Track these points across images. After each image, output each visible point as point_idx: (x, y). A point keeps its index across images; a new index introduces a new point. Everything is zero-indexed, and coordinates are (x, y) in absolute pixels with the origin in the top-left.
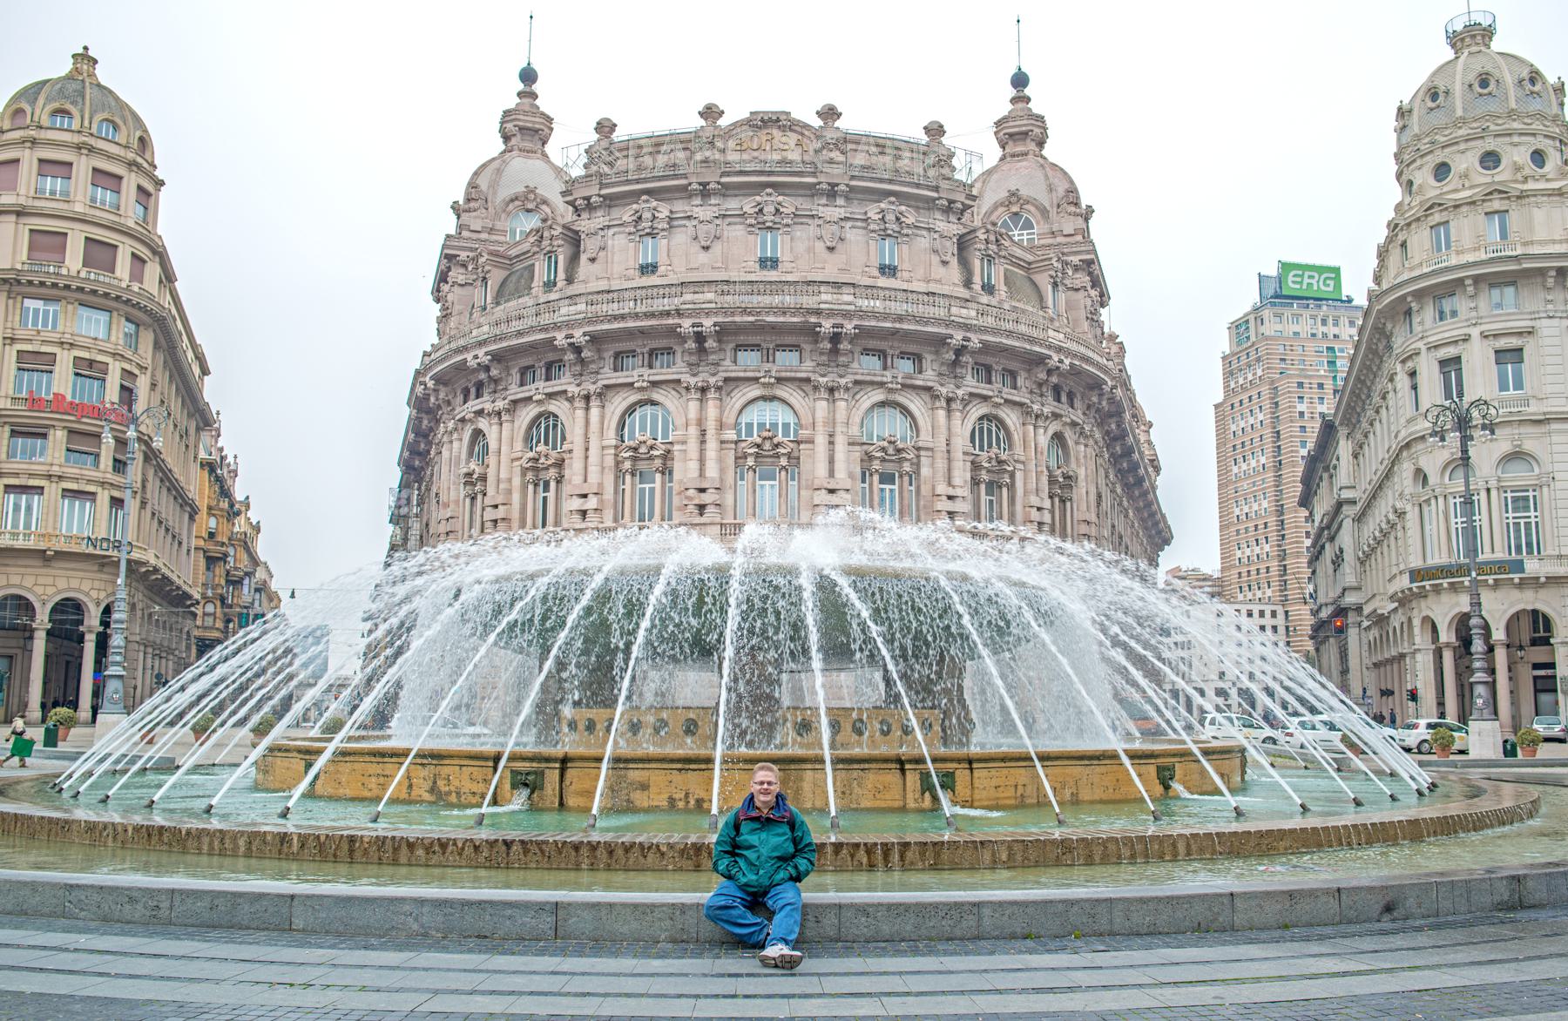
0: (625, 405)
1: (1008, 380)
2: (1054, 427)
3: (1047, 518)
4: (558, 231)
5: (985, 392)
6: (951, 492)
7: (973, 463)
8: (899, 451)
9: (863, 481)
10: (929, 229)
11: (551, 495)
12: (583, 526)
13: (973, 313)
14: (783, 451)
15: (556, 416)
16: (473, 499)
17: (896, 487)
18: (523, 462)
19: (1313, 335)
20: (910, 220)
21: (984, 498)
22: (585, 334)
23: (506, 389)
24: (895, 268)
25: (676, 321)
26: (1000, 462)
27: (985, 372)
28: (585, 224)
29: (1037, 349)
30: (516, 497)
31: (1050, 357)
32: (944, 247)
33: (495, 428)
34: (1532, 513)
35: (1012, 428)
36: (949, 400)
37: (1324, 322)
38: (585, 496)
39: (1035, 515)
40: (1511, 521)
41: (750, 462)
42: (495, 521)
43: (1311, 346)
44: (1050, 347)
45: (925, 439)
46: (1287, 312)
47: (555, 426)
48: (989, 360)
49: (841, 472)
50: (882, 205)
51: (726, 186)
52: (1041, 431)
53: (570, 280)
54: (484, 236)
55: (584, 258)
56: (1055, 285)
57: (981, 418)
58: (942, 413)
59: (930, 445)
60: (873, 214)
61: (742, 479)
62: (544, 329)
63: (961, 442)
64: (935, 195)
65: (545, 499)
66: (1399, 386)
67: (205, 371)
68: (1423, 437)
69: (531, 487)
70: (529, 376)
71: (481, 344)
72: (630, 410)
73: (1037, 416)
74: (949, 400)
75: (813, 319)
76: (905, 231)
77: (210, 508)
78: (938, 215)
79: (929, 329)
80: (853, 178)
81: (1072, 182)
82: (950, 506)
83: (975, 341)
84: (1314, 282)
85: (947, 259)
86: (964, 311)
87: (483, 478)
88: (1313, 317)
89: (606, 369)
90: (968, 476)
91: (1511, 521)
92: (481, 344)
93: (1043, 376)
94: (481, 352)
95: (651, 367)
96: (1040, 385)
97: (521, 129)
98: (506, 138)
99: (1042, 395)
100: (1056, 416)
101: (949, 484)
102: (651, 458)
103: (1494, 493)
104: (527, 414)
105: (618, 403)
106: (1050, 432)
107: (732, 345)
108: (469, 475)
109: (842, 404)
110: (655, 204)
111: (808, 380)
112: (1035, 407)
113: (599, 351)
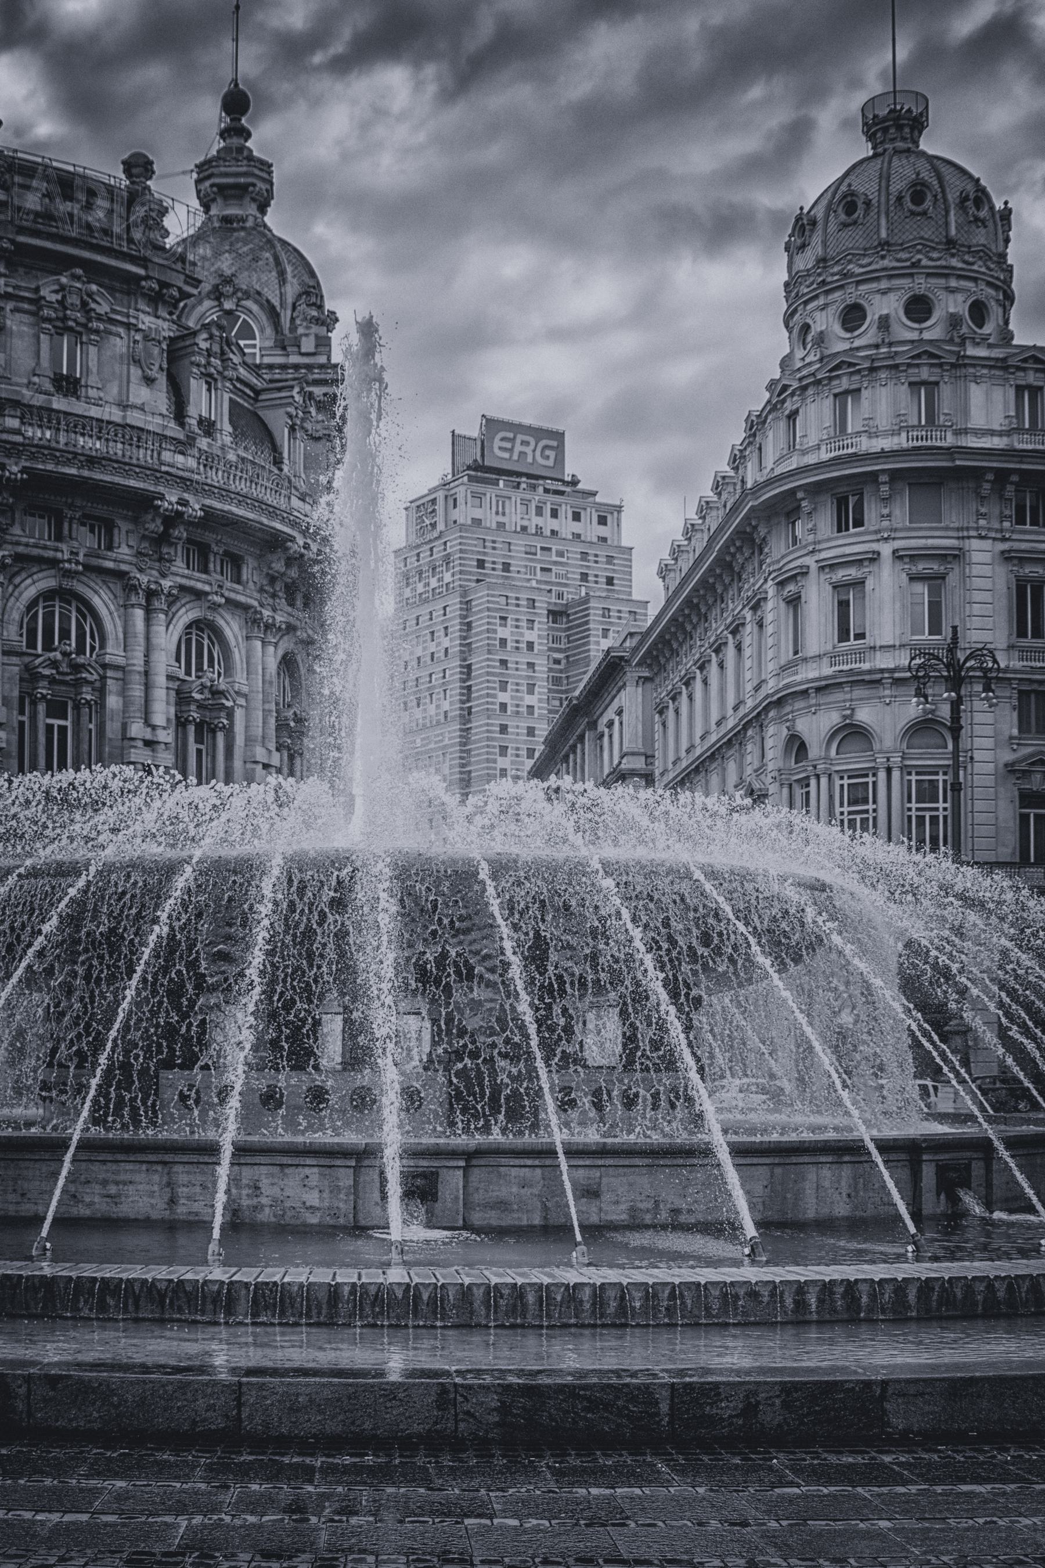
1: (228, 569)
5: (199, 586)
6: (148, 736)
7: (178, 692)
10: (128, 326)
13: (192, 463)
19: (524, 529)
20: (103, 308)
21: (192, 747)
24: (77, 381)
26: (216, 693)
27: (200, 555)
29: (279, 526)
32: (150, 355)
34: (941, 805)
35: (232, 642)
36: (151, 595)
37: (539, 512)
40: (913, 813)
43: (520, 544)
45: (114, 653)
46: (490, 492)
48: (209, 537)
50: (64, 280)
52: (271, 649)
56: (292, 429)
57: (189, 626)
58: (139, 614)
59: (121, 661)
63: (163, 663)
64: (142, 272)
66: (769, 617)
68: (805, 693)
73: (267, 627)
76: (94, 325)
78: (142, 306)
79: (132, 483)
80: (21, 230)
81: (312, 274)
83: (195, 507)
84: (528, 450)
85: (154, 373)
86: (180, 458)
88: (526, 503)
90: (172, 710)
91: (913, 813)
99: (274, 596)
101: (148, 723)
103: (896, 774)
112: (266, 613)
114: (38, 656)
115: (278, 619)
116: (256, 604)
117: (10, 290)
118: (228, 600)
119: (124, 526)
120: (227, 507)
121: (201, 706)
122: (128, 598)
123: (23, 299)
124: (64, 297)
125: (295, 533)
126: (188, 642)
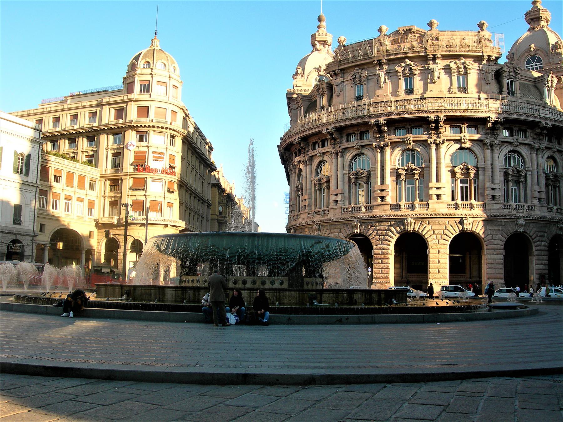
0: (352, 156)
2: (548, 154)
3: (543, 196)
4: (325, 85)
6: (493, 186)
12: (336, 207)
16: (299, 197)
17: (468, 185)
22: (333, 128)
23: (308, 151)
25: (368, 120)
26: (518, 171)
28: (335, 81)
30: (313, 195)
31: (541, 122)
32: (487, 77)
35: (525, 155)
38: (337, 195)
39: (536, 194)
41: (403, 177)
44: (540, 118)
51: (389, 60)
53: (330, 105)
55: (334, 95)
57: (509, 152)
58: (488, 152)
59: (483, 166)
60: (453, 65)
62: (318, 127)
64: (481, 54)
67: (211, 149)
70: (317, 146)
71: (297, 134)
72: (354, 158)
73: (537, 150)
74: (492, 146)
75: (425, 115)
77: (219, 203)
82: (492, 193)
87: (302, 188)
89: (344, 141)
90: (502, 179)
92: (297, 134)
93: (539, 131)
94: (297, 137)
95: (361, 139)
96: (539, 135)
97: (319, 41)
98: (314, 45)
100: (547, 148)
101: (493, 182)
102: (362, 178)
104: (316, 161)
105: (349, 156)
106: (546, 156)
107: (393, 128)
108: (298, 187)
110: (360, 71)
111: (426, 141)
112: (536, 145)
113: (341, 134)
115: (542, 146)
116: (532, 143)
118: (521, 144)
119: (481, 127)
120: (513, 117)
121: (513, 176)
122: (484, 147)
125: (541, 120)
126: (510, 157)
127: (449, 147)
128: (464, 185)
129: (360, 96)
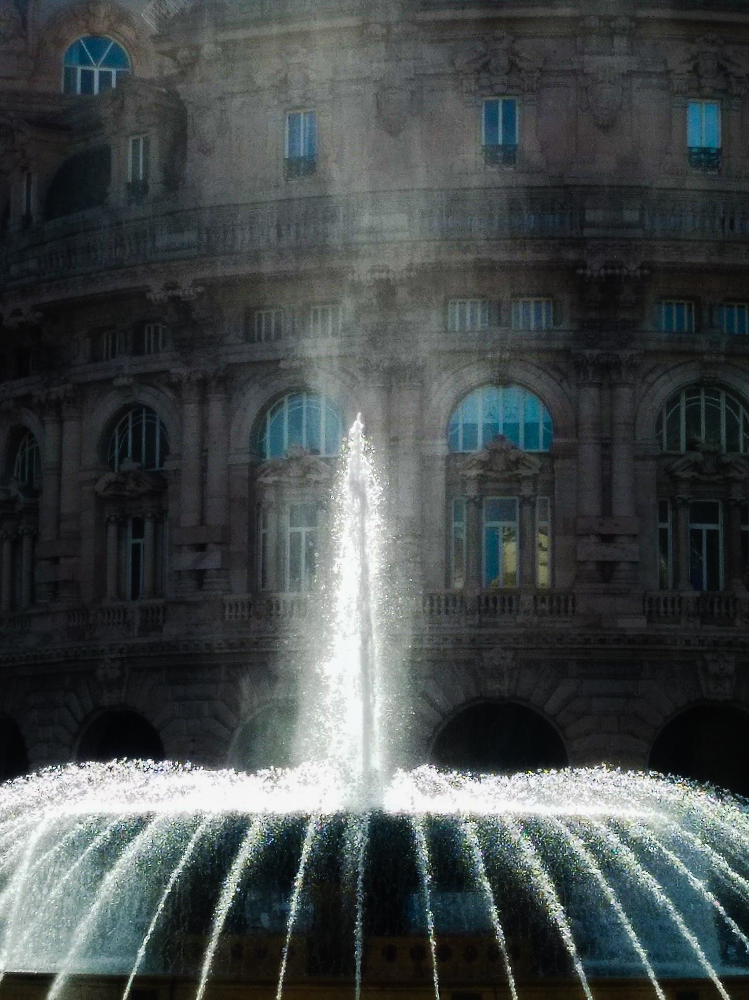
8: (722, 467)
9: (663, 519)
11: (146, 542)
14: (524, 472)
15: (150, 411)
16: (16, 544)
17: (718, 527)
18: (100, 487)
33: (51, 429)
38: (201, 547)
42: (55, 586)
47: (151, 428)
49: (623, 506)
54: (20, 85)
61: (458, 518)
65: (136, 548)
69: (112, 530)
75: (571, 255)
109: (625, 392)
114: (681, 456)
117: (635, 67)
123: (650, 74)
124: (696, 67)
127: (650, 378)
128: (705, 527)
129: (300, 159)
